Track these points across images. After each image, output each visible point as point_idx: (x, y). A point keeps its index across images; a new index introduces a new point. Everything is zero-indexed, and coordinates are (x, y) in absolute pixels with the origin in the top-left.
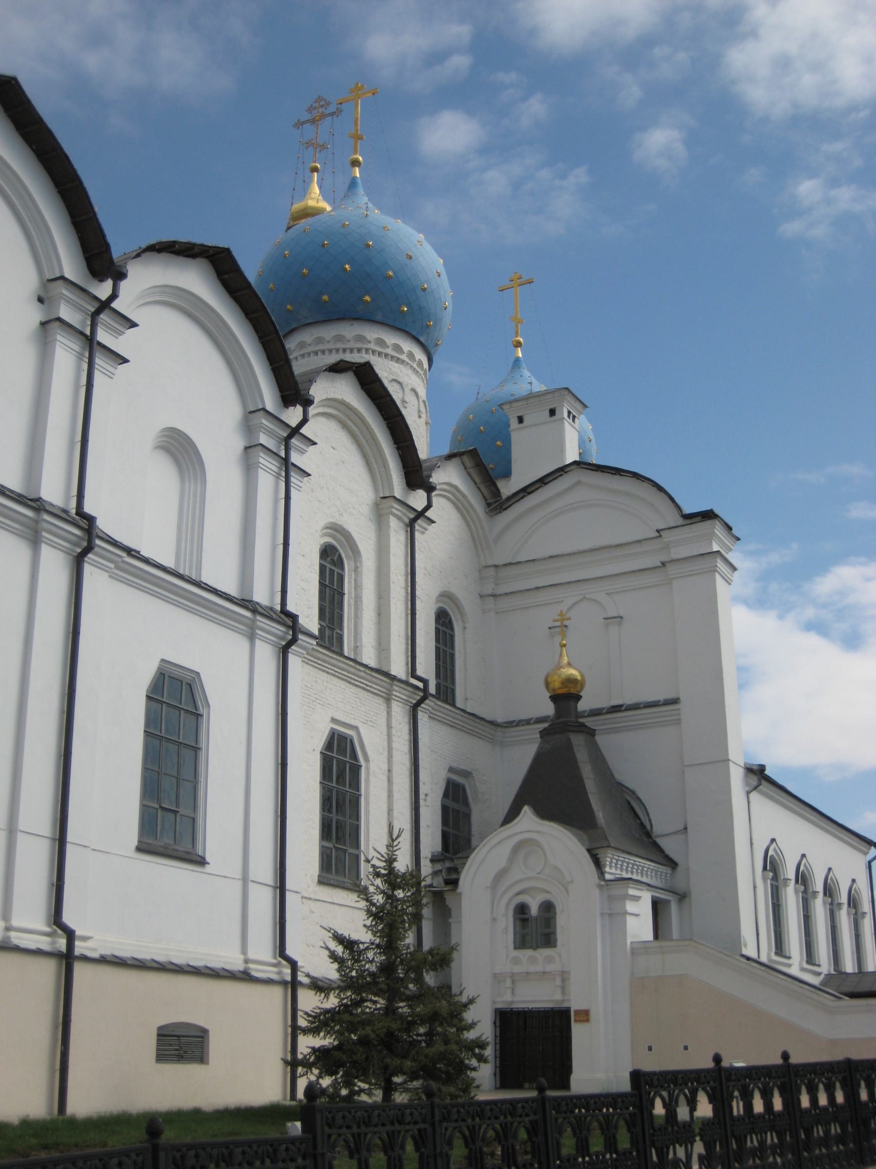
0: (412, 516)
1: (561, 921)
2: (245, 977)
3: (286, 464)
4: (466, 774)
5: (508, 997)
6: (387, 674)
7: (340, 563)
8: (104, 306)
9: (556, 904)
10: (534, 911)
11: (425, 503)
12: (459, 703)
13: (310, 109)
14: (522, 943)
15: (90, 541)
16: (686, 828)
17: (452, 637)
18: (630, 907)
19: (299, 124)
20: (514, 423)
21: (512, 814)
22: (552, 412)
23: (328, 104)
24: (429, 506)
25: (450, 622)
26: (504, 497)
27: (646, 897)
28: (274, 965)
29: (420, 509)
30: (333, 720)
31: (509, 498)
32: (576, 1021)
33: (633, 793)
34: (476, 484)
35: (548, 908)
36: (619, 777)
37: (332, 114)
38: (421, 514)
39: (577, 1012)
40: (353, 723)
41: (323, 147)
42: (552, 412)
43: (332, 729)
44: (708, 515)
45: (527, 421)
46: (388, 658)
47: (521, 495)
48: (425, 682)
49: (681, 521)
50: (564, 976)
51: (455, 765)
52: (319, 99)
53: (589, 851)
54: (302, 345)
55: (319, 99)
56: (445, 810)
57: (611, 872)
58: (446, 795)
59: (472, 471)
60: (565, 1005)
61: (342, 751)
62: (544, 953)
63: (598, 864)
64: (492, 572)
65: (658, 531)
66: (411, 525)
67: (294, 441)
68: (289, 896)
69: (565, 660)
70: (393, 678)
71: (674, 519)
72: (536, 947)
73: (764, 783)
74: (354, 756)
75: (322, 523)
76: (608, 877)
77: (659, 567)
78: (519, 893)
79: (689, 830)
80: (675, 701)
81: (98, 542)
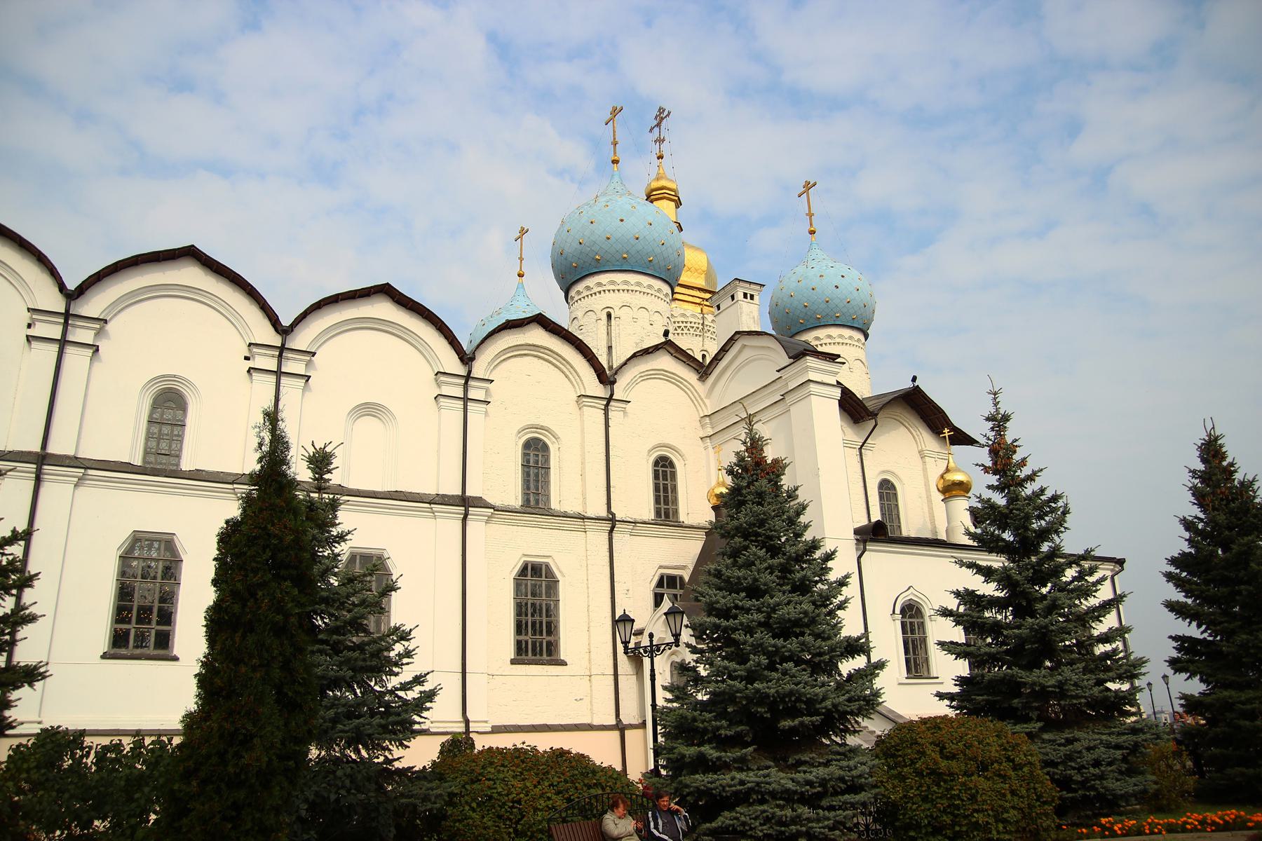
13: (656, 118)
23: (664, 111)
34: (685, 362)
37: (665, 117)
45: (722, 308)
47: (716, 362)
49: (792, 360)
55: (660, 109)
64: (707, 420)
77: (833, 385)
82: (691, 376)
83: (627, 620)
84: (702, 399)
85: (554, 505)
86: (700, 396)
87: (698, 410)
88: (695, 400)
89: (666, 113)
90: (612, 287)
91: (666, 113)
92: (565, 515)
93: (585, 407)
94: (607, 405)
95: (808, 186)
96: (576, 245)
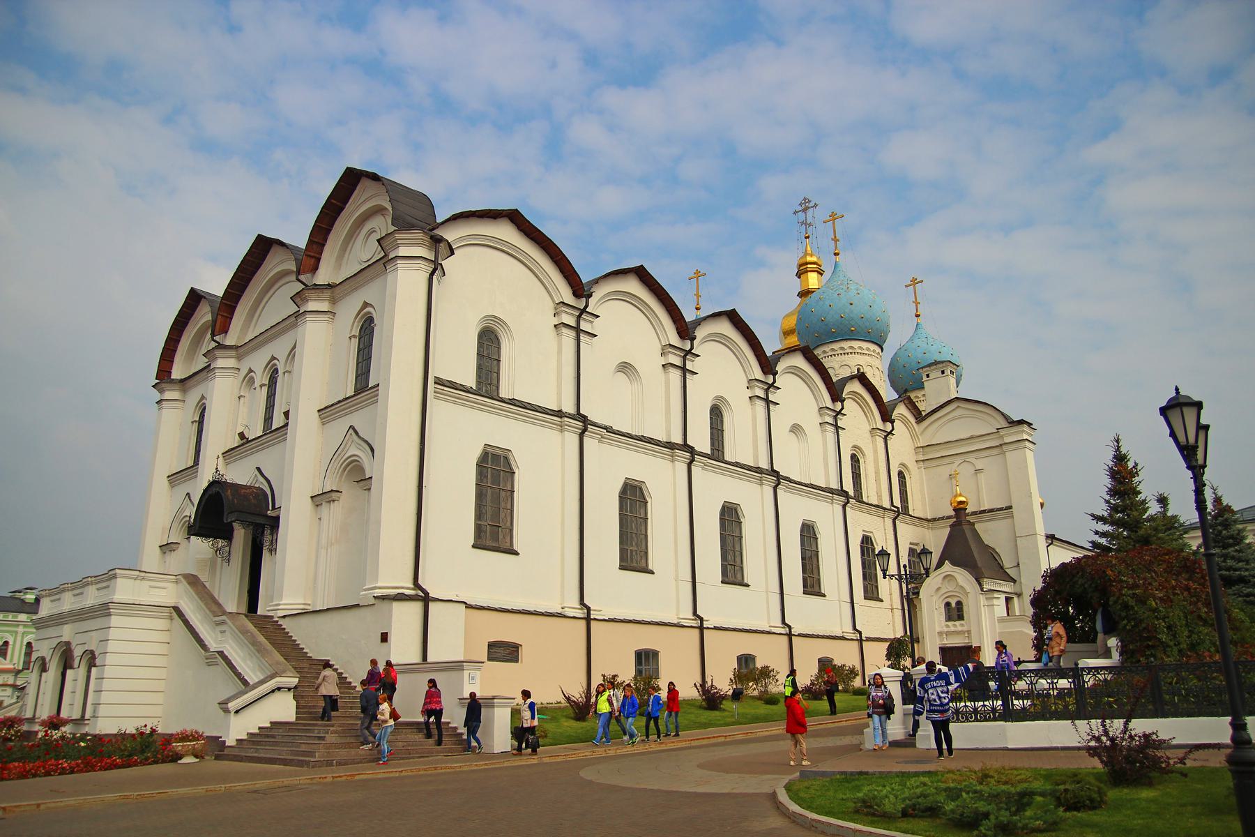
1: (965, 608)
2: (843, 638)
3: (837, 427)
6: (882, 508)
7: (858, 461)
10: (953, 605)
11: (891, 429)
13: (801, 205)
14: (949, 618)
15: (778, 480)
17: (905, 482)
18: (995, 602)
19: (795, 213)
20: (925, 378)
21: (940, 564)
22: (943, 372)
24: (893, 429)
27: (1003, 597)
28: (854, 633)
31: (925, 415)
33: (994, 549)
35: (959, 603)
36: (986, 542)
37: (812, 207)
38: (890, 433)
42: (943, 372)
44: (1021, 422)
45: (931, 377)
46: (881, 499)
48: (898, 508)
49: (1008, 425)
50: (969, 632)
51: (912, 541)
52: (805, 199)
53: (976, 579)
54: (824, 352)
55: (805, 199)
57: (986, 587)
58: (909, 555)
60: (970, 644)
61: (867, 543)
62: (957, 623)
63: (980, 585)
64: (921, 450)
65: (998, 429)
66: (885, 439)
70: (885, 509)
71: (1004, 424)
74: (872, 544)
75: (851, 446)
78: (946, 598)
80: (1010, 507)
82: (912, 420)
84: (917, 436)
85: (865, 499)
86: (916, 433)
87: (913, 442)
88: (913, 436)
89: (812, 204)
90: (860, 351)
92: (871, 505)
94: (886, 436)
95: (914, 282)
96: (838, 317)
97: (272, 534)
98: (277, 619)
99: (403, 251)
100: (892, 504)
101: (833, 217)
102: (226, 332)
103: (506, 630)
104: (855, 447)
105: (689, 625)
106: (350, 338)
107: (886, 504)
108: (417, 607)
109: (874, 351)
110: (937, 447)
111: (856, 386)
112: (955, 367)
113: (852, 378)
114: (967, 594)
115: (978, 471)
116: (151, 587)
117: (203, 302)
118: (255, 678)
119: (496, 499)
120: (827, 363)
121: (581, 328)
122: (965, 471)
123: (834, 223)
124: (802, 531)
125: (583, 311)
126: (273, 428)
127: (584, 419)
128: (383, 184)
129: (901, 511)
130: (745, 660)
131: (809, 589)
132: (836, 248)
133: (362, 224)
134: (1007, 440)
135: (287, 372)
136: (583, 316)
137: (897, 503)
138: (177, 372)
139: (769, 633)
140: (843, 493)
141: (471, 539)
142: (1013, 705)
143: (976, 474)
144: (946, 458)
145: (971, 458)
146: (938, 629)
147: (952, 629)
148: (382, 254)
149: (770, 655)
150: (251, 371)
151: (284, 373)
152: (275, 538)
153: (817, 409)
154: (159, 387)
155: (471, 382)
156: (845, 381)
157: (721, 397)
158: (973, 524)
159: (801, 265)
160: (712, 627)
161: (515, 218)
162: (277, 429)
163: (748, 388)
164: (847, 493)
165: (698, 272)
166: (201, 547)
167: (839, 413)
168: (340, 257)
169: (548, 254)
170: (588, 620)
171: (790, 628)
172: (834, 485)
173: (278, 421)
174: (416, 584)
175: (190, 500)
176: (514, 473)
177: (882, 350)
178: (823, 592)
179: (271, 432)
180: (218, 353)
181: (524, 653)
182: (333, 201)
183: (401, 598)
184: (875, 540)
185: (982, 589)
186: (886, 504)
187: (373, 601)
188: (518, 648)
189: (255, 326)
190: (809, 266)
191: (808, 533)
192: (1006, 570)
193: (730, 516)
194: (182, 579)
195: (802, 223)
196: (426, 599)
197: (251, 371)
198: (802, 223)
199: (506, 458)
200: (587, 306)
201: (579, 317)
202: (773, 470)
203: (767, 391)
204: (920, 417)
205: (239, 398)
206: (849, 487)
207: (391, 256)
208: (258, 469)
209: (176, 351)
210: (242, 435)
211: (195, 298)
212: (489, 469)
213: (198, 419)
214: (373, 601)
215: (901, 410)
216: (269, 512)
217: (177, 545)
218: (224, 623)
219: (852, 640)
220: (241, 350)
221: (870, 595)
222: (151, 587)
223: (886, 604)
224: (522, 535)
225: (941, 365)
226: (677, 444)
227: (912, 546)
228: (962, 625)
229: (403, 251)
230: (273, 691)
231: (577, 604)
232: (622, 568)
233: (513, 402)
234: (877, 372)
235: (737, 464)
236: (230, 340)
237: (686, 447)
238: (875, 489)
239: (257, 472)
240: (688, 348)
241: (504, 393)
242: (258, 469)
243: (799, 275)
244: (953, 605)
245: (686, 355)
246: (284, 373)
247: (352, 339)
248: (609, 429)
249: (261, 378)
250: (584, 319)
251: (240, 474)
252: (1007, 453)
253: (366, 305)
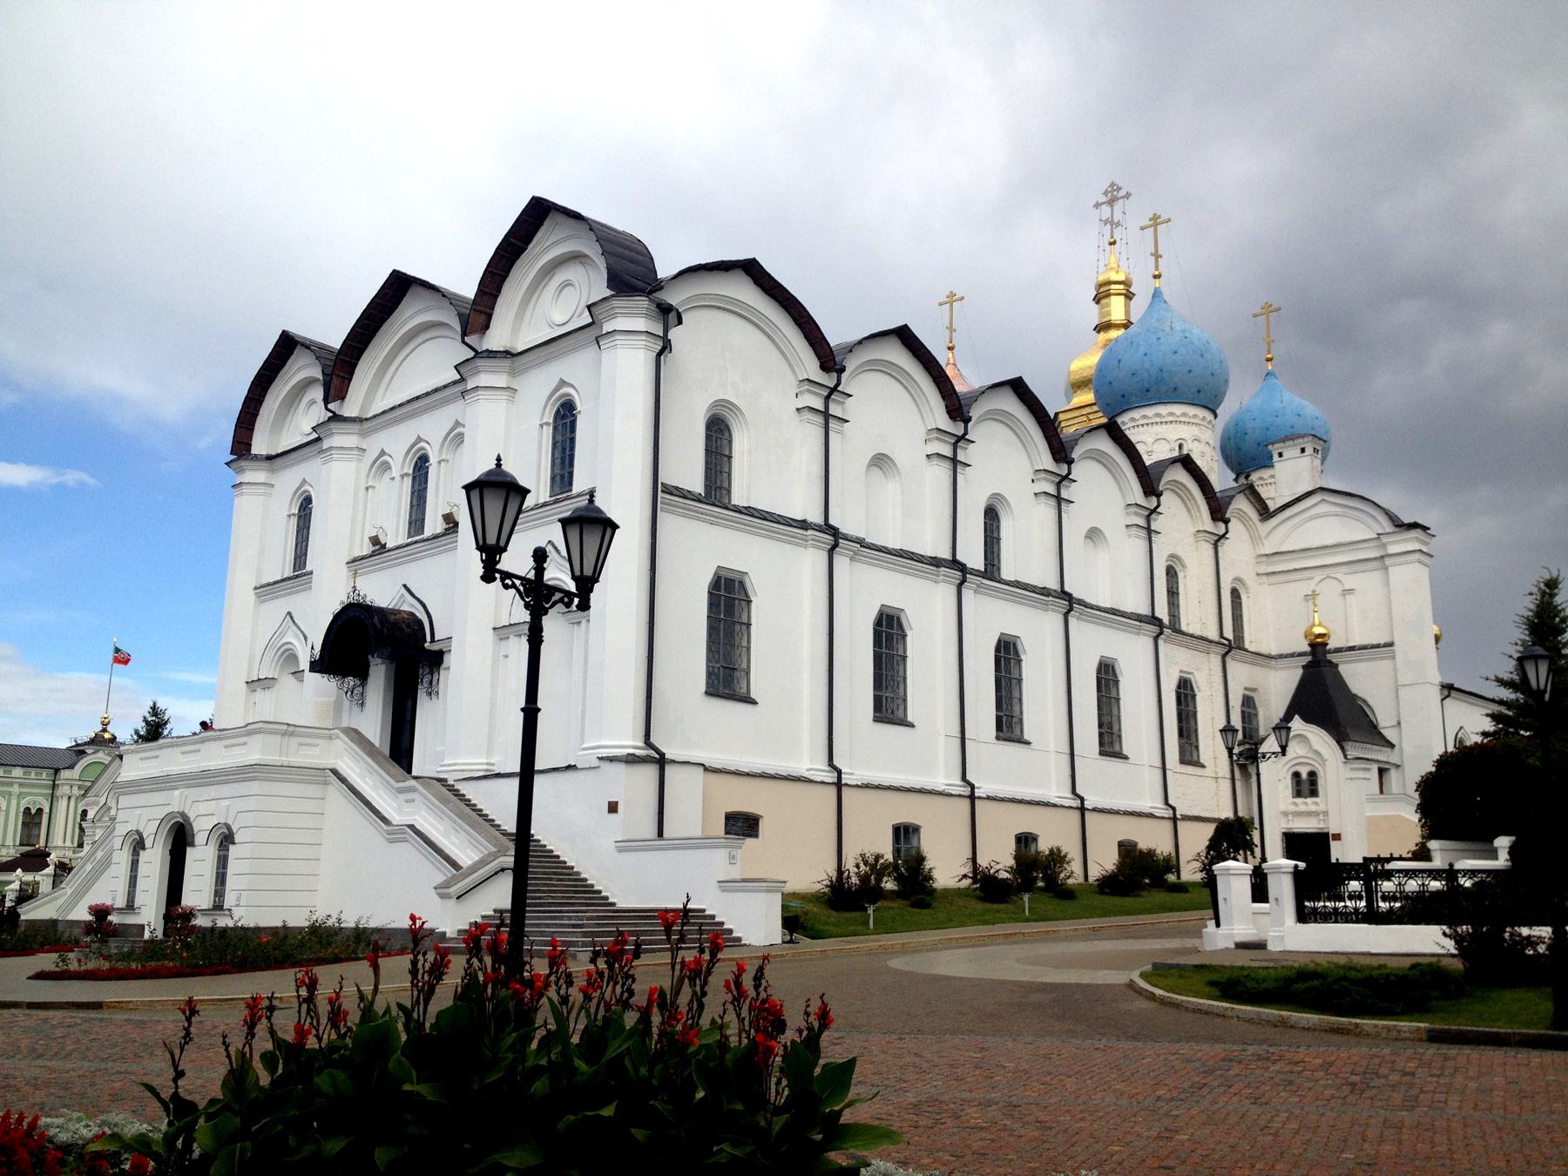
0: (1216, 538)
1: (1321, 782)
4: (1254, 690)
5: (1291, 825)
8: (1066, 477)
9: (1318, 773)
10: (1304, 776)
11: (1224, 531)
12: (1247, 646)
13: (1106, 193)
14: (1298, 793)
16: (1399, 723)
17: (1240, 604)
19: (1097, 205)
20: (1276, 457)
22: (1303, 450)
24: (1227, 532)
25: (1239, 594)
26: (1272, 510)
29: (1221, 534)
30: (1181, 671)
31: (1274, 511)
32: (1333, 840)
33: (1364, 701)
35: (1312, 774)
37: (1122, 198)
38: (1223, 536)
39: (1333, 835)
40: (1191, 671)
41: (1118, 224)
42: (1303, 450)
43: (1181, 676)
45: (1286, 455)
48: (1229, 641)
50: (1326, 813)
51: (1247, 686)
54: (1133, 419)
55: (1112, 184)
56: (1243, 712)
57: (1351, 753)
58: (1243, 705)
59: (1249, 497)
60: (1326, 831)
61: (1185, 688)
62: (1309, 800)
63: (1343, 749)
64: (1264, 559)
65: (1378, 534)
67: (1153, 516)
68: (1168, 772)
69: (1317, 622)
70: (1211, 642)
72: (1306, 798)
73: (1452, 691)
75: (1167, 555)
76: (1349, 757)
79: (1402, 721)
80: (1391, 644)
81: (1075, 605)
83: (1228, 730)
85: (1184, 628)
88: (1255, 539)
89: (1122, 193)
90: (1183, 419)
91: (1122, 193)
92: (1192, 636)
93: (1203, 542)
97: (432, 673)
98: (453, 783)
99: (621, 323)
100: (1222, 636)
101: (1156, 221)
102: (343, 398)
103: (745, 799)
104: (1173, 556)
105: (957, 793)
106: (541, 426)
107: (1214, 635)
108: (649, 773)
109: (1204, 419)
110: (1288, 557)
111: (1180, 475)
112: (1321, 442)
113: (1174, 461)
114: (1324, 761)
115: (1347, 592)
116: (301, 744)
117: (298, 350)
118: (466, 860)
119: (730, 634)
120: (1133, 435)
121: (830, 413)
122: (1329, 591)
123: (1156, 230)
124: (1099, 671)
125: (834, 390)
126: (428, 532)
127: (834, 532)
128: (591, 229)
129: (1232, 647)
130: (1025, 841)
131: (1107, 749)
132: (1157, 268)
133: (549, 272)
134: (1392, 549)
135: (442, 460)
136: (832, 397)
137: (1229, 633)
138: (259, 446)
139: (1055, 806)
140: (1154, 620)
141: (702, 687)
142: (1378, 907)
143: (1344, 595)
144: (1298, 573)
145: (1339, 573)
146: (1282, 808)
147: (1303, 808)
148: (591, 320)
149: (1054, 834)
150: (383, 453)
151: (439, 462)
152: (435, 679)
153: (1122, 505)
154: (234, 465)
155: (697, 485)
156: (1163, 465)
157: (999, 494)
158: (1337, 665)
159: (1101, 285)
160: (985, 796)
161: (752, 270)
162: (436, 537)
163: (1033, 481)
164: (1160, 621)
165: (952, 294)
166: (323, 687)
167: (1154, 511)
168: (520, 315)
169: (791, 316)
170: (839, 785)
171: (1082, 799)
172: (1144, 610)
173: (433, 525)
174: (648, 744)
175: (294, 621)
176: (751, 601)
177: (1216, 416)
178: (1125, 753)
179: (424, 540)
180: (334, 426)
181: (763, 826)
182: (512, 240)
183: (631, 760)
184: (1196, 683)
185: (1345, 756)
186: (1214, 635)
187: (596, 763)
188: (758, 820)
189: (386, 390)
190: (1113, 286)
191: (1107, 676)
192: (1382, 731)
193: (1007, 653)
194: (342, 735)
195: (1106, 222)
196: (661, 761)
197: (383, 453)
198: (1106, 222)
199: (742, 583)
200: (838, 384)
201: (827, 398)
202: (1063, 592)
203: (1058, 485)
204: (1265, 513)
205: (367, 489)
206: (1162, 613)
207: (607, 327)
208: (405, 586)
209: (257, 415)
210: (375, 541)
211: (287, 346)
212: (723, 598)
213: (297, 512)
214: (596, 763)
215: (1241, 504)
216: (426, 645)
217: (272, 681)
218: (412, 790)
219: (1163, 818)
220: (367, 425)
221: (1188, 757)
222: (301, 744)
223: (1208, 772)
224: (760, 679)
225: (1300, 440)
226: (943, 559)
227: (1247, 693)
228: (1317, 804)
229: (621, 323)
230: (496, 873)
231: (824, 766)
232: (876, 719)
233: (750, 512)
234: (1208, 450)
235: (1017, 584)
236: (350, 408)
237: (955, 564)
238: (1198, 615)
239: (404, 591)
240: (960, 433)
241: (738, 498)
242: (405, 586)
243: (1097, 300)
244: (1304, 776)
245: (957, 442)
246: (439, 462)
247: (545, 427)
248: (861, 542)
249: (401, 465)
250: (834, 400)
251: (381, 591)
252: (1390, 569)
253: (563, 383)
